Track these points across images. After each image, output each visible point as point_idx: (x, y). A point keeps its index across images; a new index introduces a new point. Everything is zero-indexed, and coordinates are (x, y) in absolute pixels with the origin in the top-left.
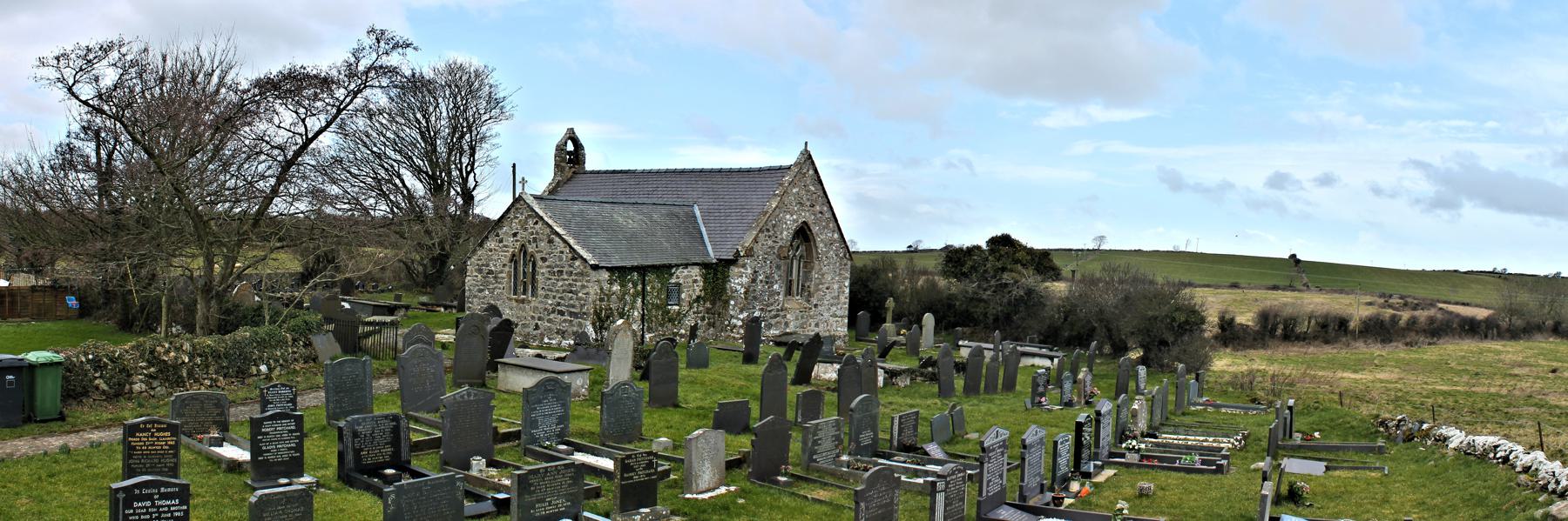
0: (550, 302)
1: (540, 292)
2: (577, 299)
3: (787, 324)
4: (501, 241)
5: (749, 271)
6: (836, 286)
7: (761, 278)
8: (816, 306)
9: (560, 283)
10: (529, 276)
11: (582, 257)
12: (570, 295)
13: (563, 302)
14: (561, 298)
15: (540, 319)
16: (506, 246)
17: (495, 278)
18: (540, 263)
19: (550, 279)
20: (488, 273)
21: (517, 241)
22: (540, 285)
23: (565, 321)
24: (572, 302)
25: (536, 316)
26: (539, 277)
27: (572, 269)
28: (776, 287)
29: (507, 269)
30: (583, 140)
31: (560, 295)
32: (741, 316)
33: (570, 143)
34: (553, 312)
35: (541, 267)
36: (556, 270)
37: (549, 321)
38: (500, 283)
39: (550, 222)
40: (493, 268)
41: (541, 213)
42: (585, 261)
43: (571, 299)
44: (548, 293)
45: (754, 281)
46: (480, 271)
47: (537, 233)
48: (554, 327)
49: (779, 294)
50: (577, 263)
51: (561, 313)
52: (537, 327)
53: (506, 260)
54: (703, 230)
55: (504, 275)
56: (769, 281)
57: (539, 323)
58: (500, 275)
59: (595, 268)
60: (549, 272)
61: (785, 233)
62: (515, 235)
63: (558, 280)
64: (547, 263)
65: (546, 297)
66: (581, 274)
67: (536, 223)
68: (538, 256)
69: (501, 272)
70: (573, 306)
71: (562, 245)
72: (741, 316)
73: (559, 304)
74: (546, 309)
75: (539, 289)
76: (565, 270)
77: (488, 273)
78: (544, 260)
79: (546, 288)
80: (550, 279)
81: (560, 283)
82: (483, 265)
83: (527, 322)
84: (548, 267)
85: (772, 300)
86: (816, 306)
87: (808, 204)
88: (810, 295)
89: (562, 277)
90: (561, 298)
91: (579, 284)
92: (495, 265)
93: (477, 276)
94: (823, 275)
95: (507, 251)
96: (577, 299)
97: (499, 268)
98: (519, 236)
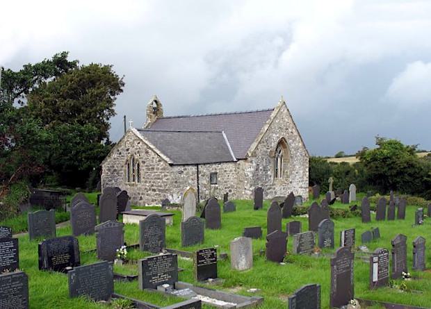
1: (142, 180)
3: (276, 193)
5: (254, 164)
6: (301, 172)
7: (261, 168)
8: (291, 182)
9: (153, 175)
10: (136, 172)
11: (164, 160)
14: (154, 182)
15: (142, 194)
18: (141, 164)
22: (142, 176)
23: (157, 194)
26: (141, 172)
28: (269, 173)
29: (124, 168)
30: (161, 101)
32: (251, 189)
33: (154, 103)
34: (150, 190)
35: (142, 166)
39: (146, 142)
41: (141, 138)
42: (166, 162)
45: (257, 170)
47: (140, 148)
48: (150, 198)
49: (271, 176)
50: (162, 163)
51: (154, 190)
54: (228, 144)
56: (265, 170)
59: (171, 165)
61: (273, 144)
62: (128, 150)
65: (146, 182)
66: (164, 169)
67: (139, 143)
68: (140, 160)
69: (121, 170)
70: (161, 186)
71: (153, 154)
72: (251, 189)
73: (153, 186)
74: (146, 189)
78: (144, 162)
81: (153, 175)
85: (267, 180)
86: (291, 182)
87: (285, 128)
88: (288, 177)
90: (154, 182)
91: (163, 174)
92: (117, 167)
94: (294, 166)
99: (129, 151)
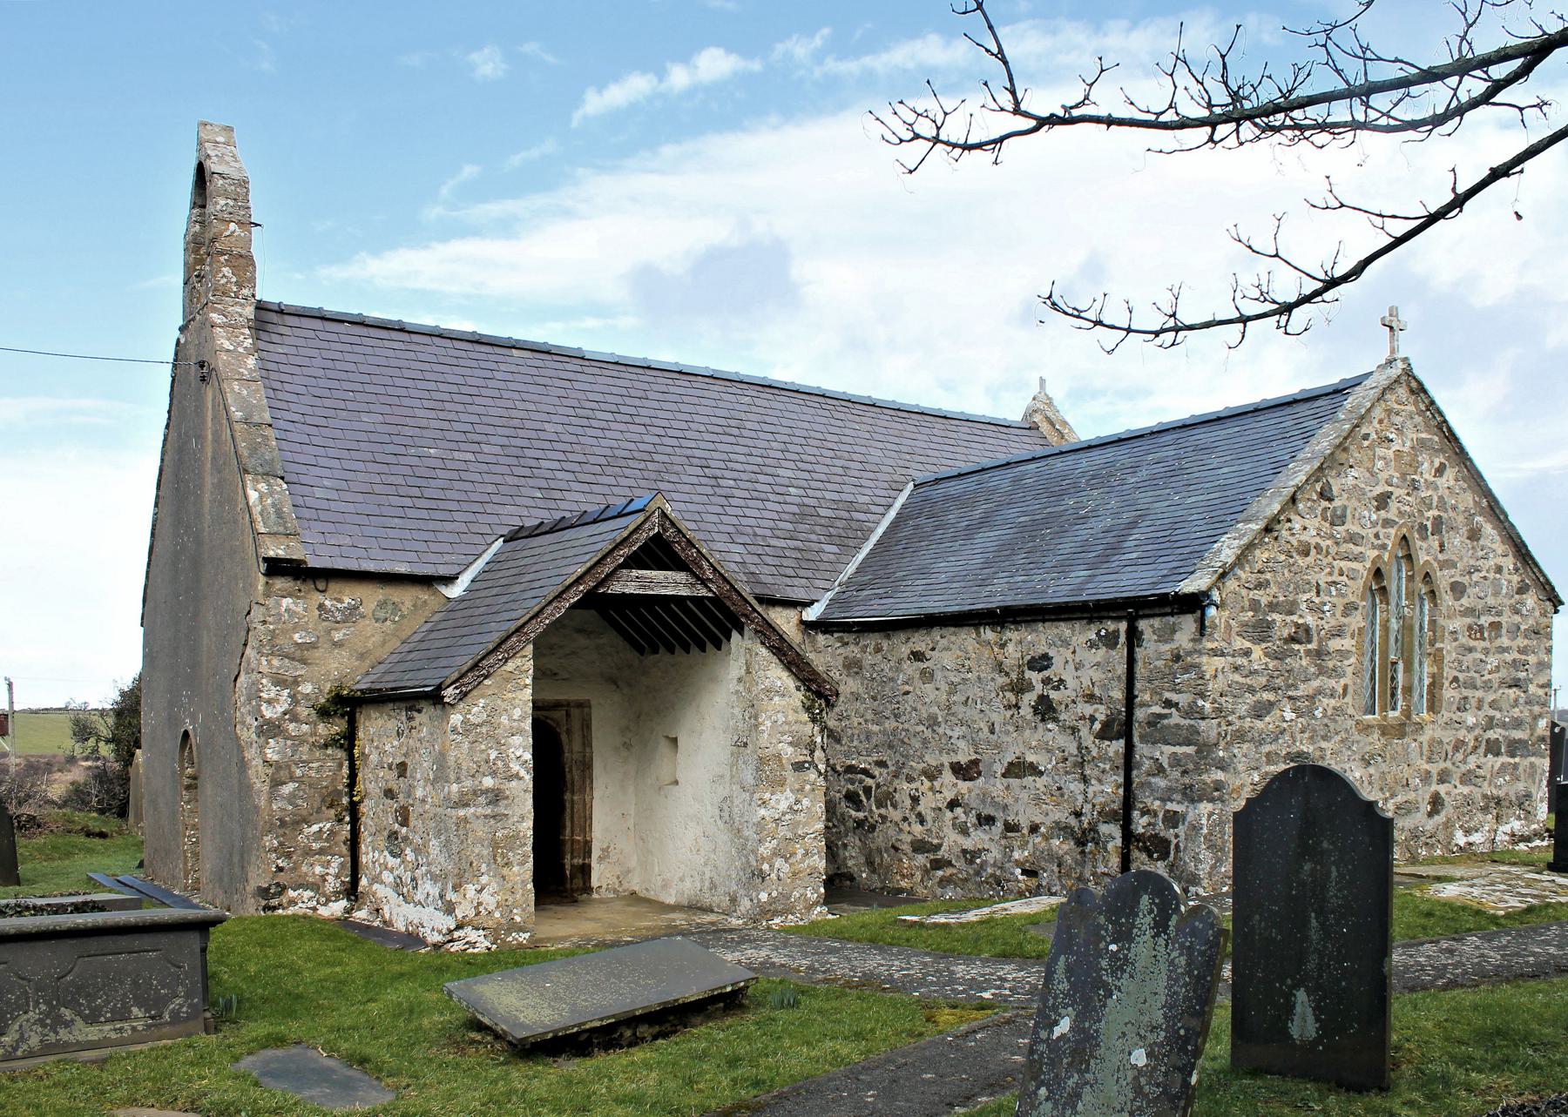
2: (1528, 702)
4: (1338, 519)
12: (1513, 692)
13: (1498, 715)
15: (1443, 778)
16: (1353, 538)
17: (1319, 654)
18: (1447, 599)
19: (1470, 650)
20: (1293, 639)
21: (1387, 523)
24: (1516, 712)
25: (1434, 769)
27: (1517, 618)
29: (1356, 621)
31: (1490, 697)
36: (1485, 620)
37: (1467, 778)
38: (1335, 673)
40: (1310, 620)
43: (1516, 703)
44: (1466, 692)
46: (1261, 631)
51: (1493, 748)
52: (1436, 803)
53: (1354, 590)
55: (1347, 643)
57: (1442, 789)
58: (1334, 644)
60: (1470, 628)
62: (1383, 501)
63: (1486, 651)
64: (1464, 601)
68: (1443, 579)
69: (1338, 633)
73: (1490, 723)
75: (1446, 684)
76: (1504, 620)
77: (1293, 639)
78: (1458, 589)
79: (1461, 676)
80: (1470, 650)
81: (1493, 661)
82: (1273, 607)
83: (1411, 796)
84: (1470, 612)
89: (1498, 643)
90: (1493, 705)
91: (1532, 659)
95: (1357, 558)
96: (1528, 702)
97: (1330, 622)
98: (1393, 505)
99: (1392, 513)
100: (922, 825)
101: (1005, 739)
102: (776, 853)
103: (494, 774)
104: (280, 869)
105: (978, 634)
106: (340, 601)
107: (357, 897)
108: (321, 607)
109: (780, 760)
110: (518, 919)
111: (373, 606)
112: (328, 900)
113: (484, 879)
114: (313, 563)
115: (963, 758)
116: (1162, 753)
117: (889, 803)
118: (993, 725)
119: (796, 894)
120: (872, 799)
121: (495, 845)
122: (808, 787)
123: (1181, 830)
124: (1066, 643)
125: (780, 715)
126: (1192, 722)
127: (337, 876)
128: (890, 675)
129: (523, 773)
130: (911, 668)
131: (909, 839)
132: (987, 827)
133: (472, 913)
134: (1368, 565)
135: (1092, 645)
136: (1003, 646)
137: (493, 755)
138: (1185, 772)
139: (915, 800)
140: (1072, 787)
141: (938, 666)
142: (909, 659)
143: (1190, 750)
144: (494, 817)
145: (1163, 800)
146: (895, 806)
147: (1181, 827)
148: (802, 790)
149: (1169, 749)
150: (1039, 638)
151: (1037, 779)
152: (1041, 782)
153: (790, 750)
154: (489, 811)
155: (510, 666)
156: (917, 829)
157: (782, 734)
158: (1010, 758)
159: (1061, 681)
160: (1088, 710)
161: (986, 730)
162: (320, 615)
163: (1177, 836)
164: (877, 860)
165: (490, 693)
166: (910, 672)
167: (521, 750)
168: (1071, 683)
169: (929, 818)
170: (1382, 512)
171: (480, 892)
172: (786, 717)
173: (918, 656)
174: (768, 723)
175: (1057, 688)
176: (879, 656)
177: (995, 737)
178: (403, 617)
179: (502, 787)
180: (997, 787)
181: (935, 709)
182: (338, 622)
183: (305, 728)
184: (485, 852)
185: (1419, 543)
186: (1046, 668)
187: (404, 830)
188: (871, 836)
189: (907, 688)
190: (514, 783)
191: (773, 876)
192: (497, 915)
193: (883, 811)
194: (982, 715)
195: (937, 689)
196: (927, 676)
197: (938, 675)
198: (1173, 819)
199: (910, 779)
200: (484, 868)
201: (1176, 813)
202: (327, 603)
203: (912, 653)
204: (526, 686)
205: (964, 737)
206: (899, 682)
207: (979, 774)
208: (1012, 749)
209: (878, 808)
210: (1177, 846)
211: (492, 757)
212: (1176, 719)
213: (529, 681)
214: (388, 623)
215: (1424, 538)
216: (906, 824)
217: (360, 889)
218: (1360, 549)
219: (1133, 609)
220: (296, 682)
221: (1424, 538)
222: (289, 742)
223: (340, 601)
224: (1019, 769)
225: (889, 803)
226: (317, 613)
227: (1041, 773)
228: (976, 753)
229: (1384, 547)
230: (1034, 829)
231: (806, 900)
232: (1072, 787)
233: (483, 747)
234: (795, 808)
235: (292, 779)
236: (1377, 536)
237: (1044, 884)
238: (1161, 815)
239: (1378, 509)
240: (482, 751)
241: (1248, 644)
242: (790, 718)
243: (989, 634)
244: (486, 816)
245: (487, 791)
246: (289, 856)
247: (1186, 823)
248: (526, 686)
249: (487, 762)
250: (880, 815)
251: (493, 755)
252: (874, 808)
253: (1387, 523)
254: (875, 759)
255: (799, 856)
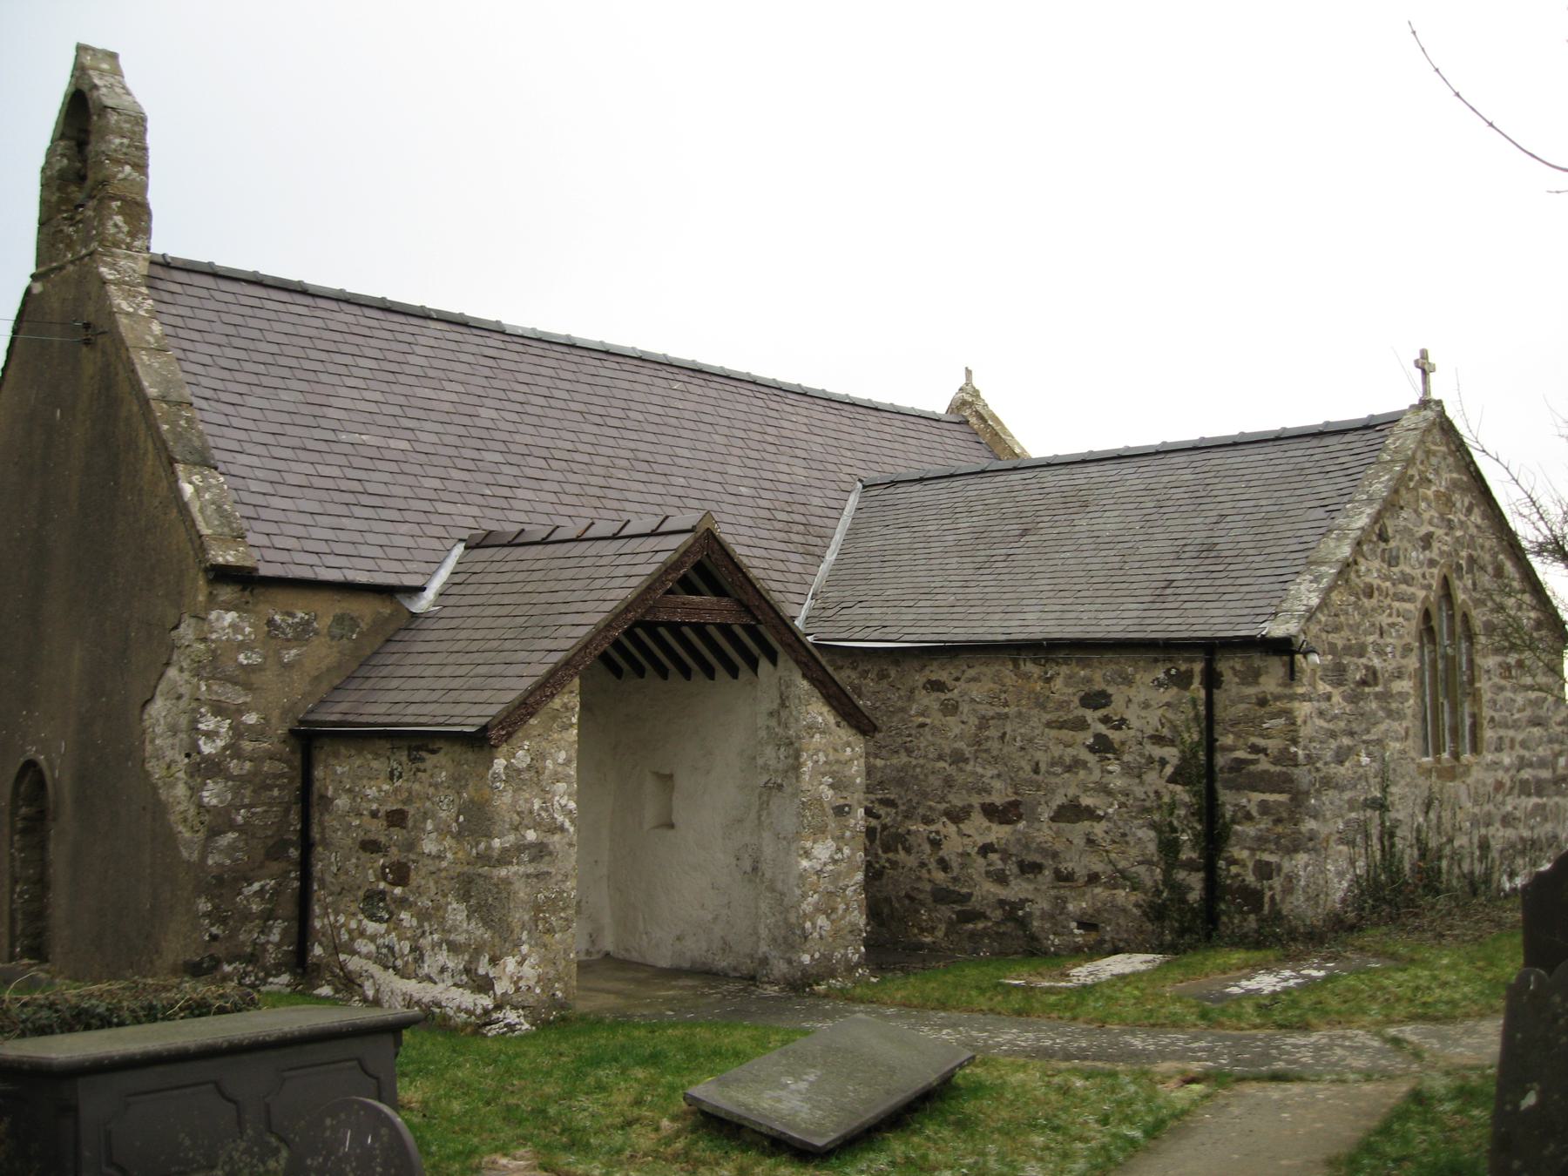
0: (1507, 761)
16: (1407, 579)
20: (1364, 683)
21: (1432, 563)
40: (1376, 662)
46: (1337, 674)
55: (1405, 685)
69: (1399, 675)
77: (1364, 683)
82: (1348, 649)
93: (1328, 697)
95: (1411, 599)
97: (1391, 665)
98: (1435, 545)
100: (946, 872)
101: (1053, 780)
102: (818, 909)
103: (536, 826)
104: (214, 938)
105: (1016, 666)
106: (292, 615)
107: (305, 969)
108: (271, 622)
109: (822, 805)
110: (559, 994)
111: (328, 620)
112: (268, 975)
113: (525, 948)
114: (265, 570)
115: (997, 799)
116: (1249, 801)
117: (900, 847)
118: (1037, 764)
119: (838, 955)
120: (878, 842)
121: (537, 908)
122: (848, 834)
123: (1277, 882)
124: (1128, 681)
125: (821, 754)
126: (1284, 769)
127: (278, 945)
128: (900, 704)
129: (567, 824)
130: (930, 700)
131: (928, 887)
132: (1031, 876)
133: (511, 990)
134: (1419, 604)
135: (1160, 684)
136: (1048, 680)
137: (537, 805)
138: (1278, 821)
139: (936, 844)
140: (1140, 833)
141: (966, 698)
142: (924, 687)
143: (1283, 798)
144: (537, 876)
145: (1252, 850)
146: (908, 850)
147: (1276, 879)
148: (842, 837)
149: (1257, 797)
150: (1098, 675)
151: (1095, 824)
152: (1099, 829)
153: (830, 793)
154: (531, 869)
155: (557, 703)
156: (940, 876)
157: (824, 775)
158: (1059, 800)
159: (1123, 721)
160: (1158, 752)
161: (1028, 768)
162: (269, 632)
163: (1271, 888)
164: (886, 910)
165: (536, 733)
166: (926, 701)
167: (566, 797)
168: (1135, 723)
169: (955, 865)
170: (1427, 552)
171: (521, 963)
172: (827, 756)
173: (937, 686)
174: (810, 764)
175: (1118, 728)
176: (884, 684)
177: (1040, 778)
178: (361, 634)
179: (545, 840)
180: (1045, 832)
181: (961, 745)
182: (288, 640)
183: (248, 765)
184: (526, 917)
185: (1457, 582)
186: (1104, 706)
187: (398, 891)
188: (877, 883)
189: (921, 719)
190: (557, 837)
191: (816, 935)
192: (538, 991)
193: (891, 855)
194: (1022, 753)
195: (963, 722)
196: (950, 709)
197: (965, 708)
198: (1264, 871)
199: (927, 821)
200: (525, 936)
201: (1268, 864)
202: (277, 618)
203: (929, 681)
204: (571, 725)
205: (999, 776)
206: (913, 712)
207: (1020, 817)
208: (1062, 791)
209: (885, 852)
210: (1272, 898)
211: (536, 807)
212: (1264, 764)
213: (574, 720)
214: (345, 641)
215: (1460, 578)
216: (924, 871)
217: (310, 960)
218: (1412, 590)
219: (1212, 648)
220: (240, 710)
221: (1460, 578)
222: (230, 783)
223: (292, 615)
224: (1072, 812)
225: (900, 847)
226: (266, 629)
227: (1100, 819)
228: (1016, 793)
229: (1429, 587)
230: (1093, 878)
231: (848, 961)
232: (1140, 833)
233: (527, 796)
234: (836, 857)
235: (232, 826)
236: (1424, 576)
237: (1107, 938)
238: (1251, 865)
239: (1424, 548)
240: (526, 801)
241: (1329, 689)
242: (831, 758)
243: (1029, 667)
244: (528, 876)
245: (531, 845)
246: (223, 921)
247: (1282, 875)
248: (571, 725)
249: (531, 812)
250: (888, 860)
251: (537, 805)
252: (880, 852)
253: (1432, 563)
254: (879, 797)
255: (840, 912)
